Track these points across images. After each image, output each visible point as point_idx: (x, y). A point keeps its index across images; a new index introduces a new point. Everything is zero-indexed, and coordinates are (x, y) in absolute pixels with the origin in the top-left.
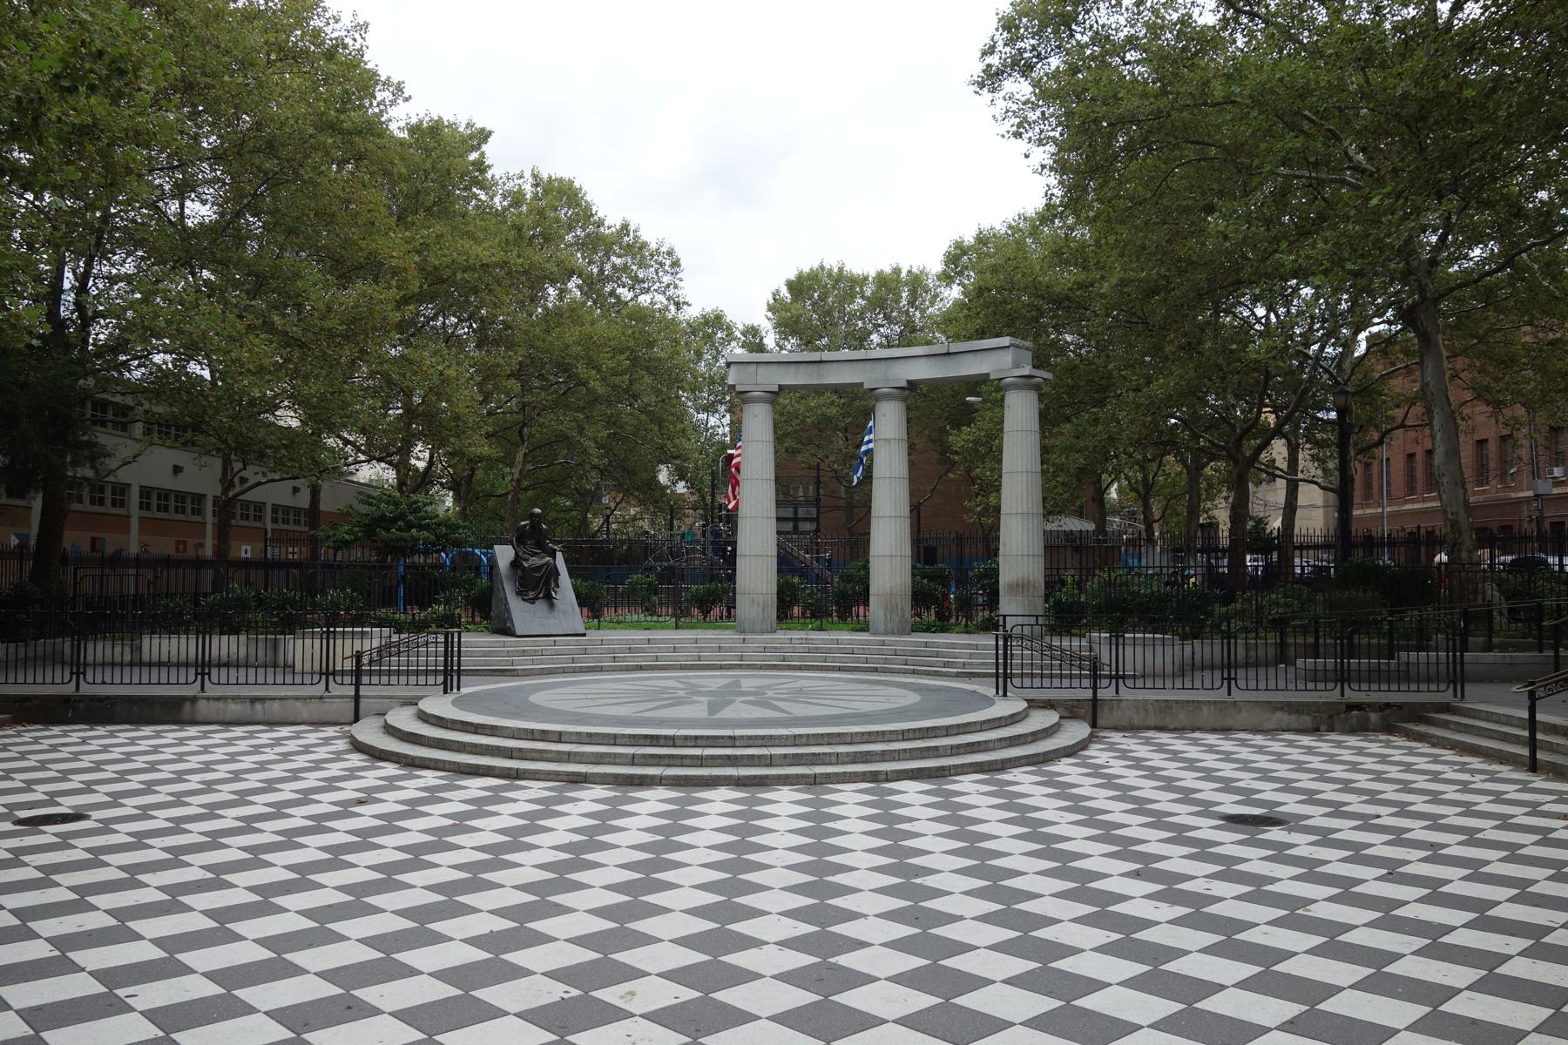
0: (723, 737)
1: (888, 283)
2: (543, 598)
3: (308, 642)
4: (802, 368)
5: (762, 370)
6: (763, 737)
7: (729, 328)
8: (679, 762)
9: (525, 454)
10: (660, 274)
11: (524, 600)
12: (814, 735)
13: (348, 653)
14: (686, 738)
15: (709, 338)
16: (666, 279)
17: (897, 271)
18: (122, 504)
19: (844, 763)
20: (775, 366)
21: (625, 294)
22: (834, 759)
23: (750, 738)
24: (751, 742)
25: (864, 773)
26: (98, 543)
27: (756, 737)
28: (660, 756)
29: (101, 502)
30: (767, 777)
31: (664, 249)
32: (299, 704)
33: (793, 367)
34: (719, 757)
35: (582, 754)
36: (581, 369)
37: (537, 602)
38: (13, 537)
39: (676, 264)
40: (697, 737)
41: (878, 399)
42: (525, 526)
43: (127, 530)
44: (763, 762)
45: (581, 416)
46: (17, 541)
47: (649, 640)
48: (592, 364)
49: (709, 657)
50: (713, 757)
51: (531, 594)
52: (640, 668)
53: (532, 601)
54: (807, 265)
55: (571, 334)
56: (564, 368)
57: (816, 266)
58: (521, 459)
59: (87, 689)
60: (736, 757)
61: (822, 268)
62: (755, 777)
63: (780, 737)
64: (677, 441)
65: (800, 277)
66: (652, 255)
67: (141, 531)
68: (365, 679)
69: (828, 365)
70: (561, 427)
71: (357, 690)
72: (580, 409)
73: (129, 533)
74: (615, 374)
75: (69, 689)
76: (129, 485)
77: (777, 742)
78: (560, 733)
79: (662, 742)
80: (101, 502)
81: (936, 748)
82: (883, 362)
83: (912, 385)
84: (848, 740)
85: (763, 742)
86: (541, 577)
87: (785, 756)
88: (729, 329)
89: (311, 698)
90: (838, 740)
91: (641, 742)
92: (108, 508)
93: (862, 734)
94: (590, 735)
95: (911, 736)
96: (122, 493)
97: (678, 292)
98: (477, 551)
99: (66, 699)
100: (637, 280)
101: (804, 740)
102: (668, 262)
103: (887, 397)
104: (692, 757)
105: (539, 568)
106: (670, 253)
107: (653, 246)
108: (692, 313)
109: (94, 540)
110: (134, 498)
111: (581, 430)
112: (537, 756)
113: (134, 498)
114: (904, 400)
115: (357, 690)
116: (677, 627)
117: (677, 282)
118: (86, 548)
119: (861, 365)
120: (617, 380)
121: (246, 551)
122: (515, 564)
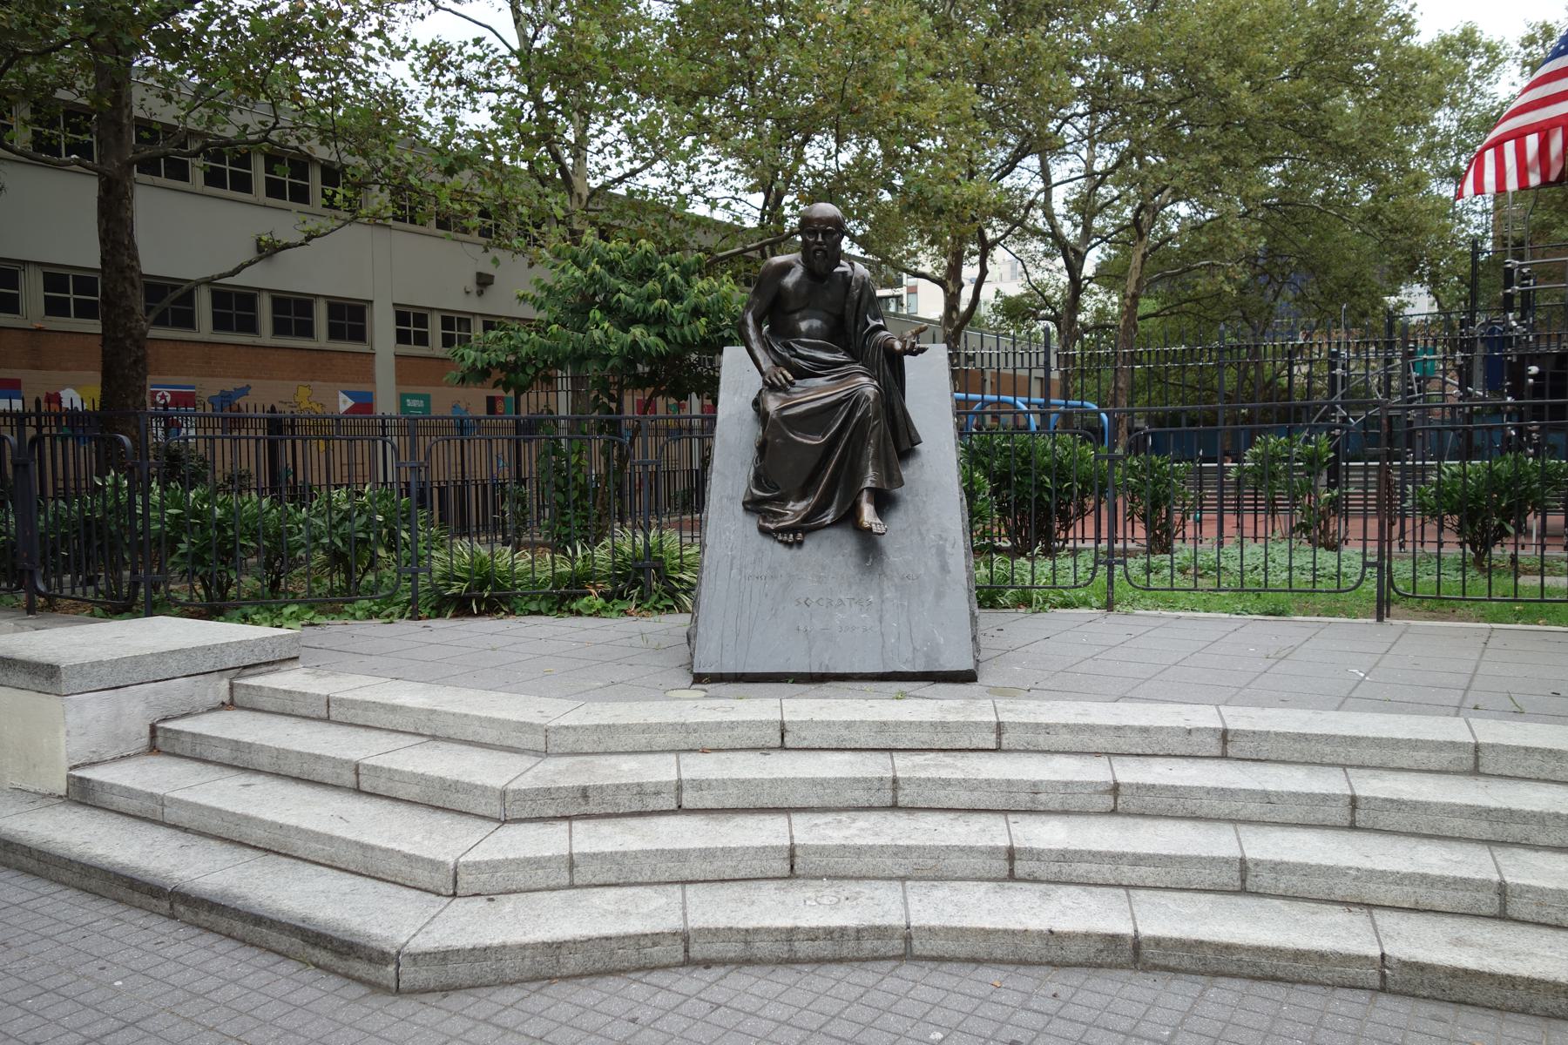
2: (833, 524)
9: (1145, 256)
11: (764, 531)
37: (811, 544)
38: (342, 397)
42: (786, 269)
46: (350, 403)
47: (1224, 736)
51: (796, 509)
53: (794, 535)
58: (1138, 264)
86: (830, 446)
88: (1493, 54)
108: (1425, 36)
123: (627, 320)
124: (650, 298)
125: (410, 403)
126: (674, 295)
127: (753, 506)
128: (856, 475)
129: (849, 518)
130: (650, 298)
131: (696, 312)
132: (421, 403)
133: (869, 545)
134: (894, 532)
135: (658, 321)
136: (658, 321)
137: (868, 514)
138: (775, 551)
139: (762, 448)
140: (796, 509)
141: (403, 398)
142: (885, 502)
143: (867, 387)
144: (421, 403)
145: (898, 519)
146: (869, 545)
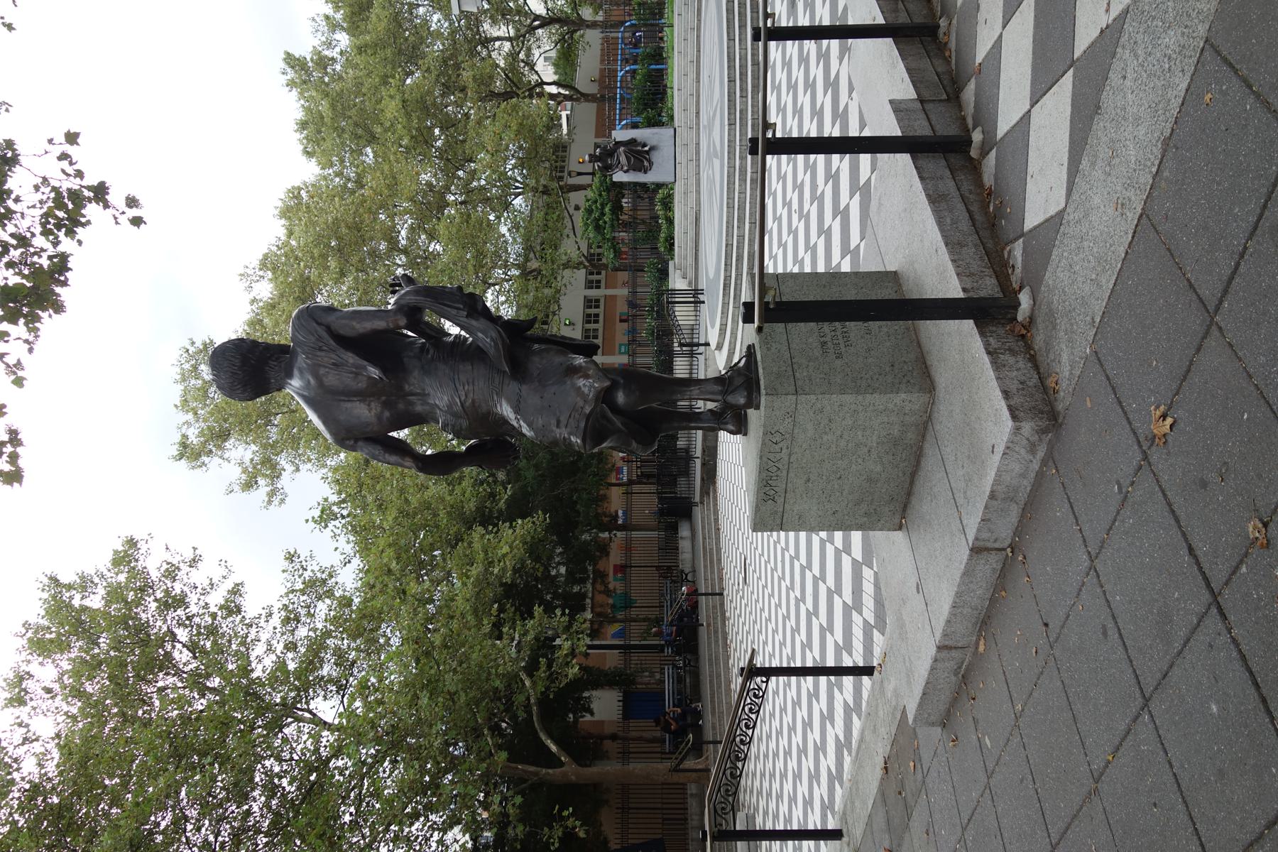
0: (726, 251)
3: (678, 318)
6: (727, 227)
8: (739, 286)
12: (728, 195)
13: (679, 349)
14: (726, 270)
18: (597, 301)
19: (746, 189)
22: (742, 196)
23: (727, 235)
24: (730, 234)
25: (751, 189)
26: (623, 318)
27: (727, 231)
28: (735, 295)
29: (597, 315)
30: (749, 252)
32: (709, 370)
34: (737, 265)
35: (732, 329)
40: (726, 265)
42: (598, 166)
43: (615, 297)
44: (741, 241)
49: (692, 52)
50: (737, 269)
51: (646, 163)
52: (698, 113)
53: (651, 163)
59: (699, 453)
60: (737, 256)
62: (748, 259)
63: (728, 217)
67: (615, 287)
68: (695, 340)
71: (702, 345)
73: (616, 296)
75: (698, 463)
76: (585, 297)
77: (731, 219)
78: (721, 325)
79: (728, 282)
80: (597, 315)
81: (741, 111)
84: (732, 170)
85: (730, 227)
86: (634, 156)
87: (738, 227)
89: (706, 364)
90: (732, 177)
91: (727, 291)
92: (601, 311)
93: (729, 158)
94: (722, 313)
95: (733, 117)
96: (590, 301)
98: (620, 74)
99: (703, 465)
101: (731, 201)
104: (736, 279)
109: (621, 321)
110: (593, 293)
112: (732, 345)
113: (593, 293)
115: (702, 345)
116: (672, 26)
118: (625, 325)
121: (625, 202)
123: (603, 214)
124: (597, 207)
125: (623, 350)
126: (596, 202)
127: (645, 172)
128: (639, 151)
129: (647, 152)
130: (597, 207)
131: (600, 195)
132: (623, 347)
133: (652, 148)
134: (651, 142)
135: (603, 206)
136: (603, 206)
137: (646, 149)
138: (654, 167)
139: (634, 170)
140: (646, 163)
141: (620, 353)
142: (645, 145)
143: (622, 149)
144: (623, 347)
145: (648, 142)
146: (652, 148)
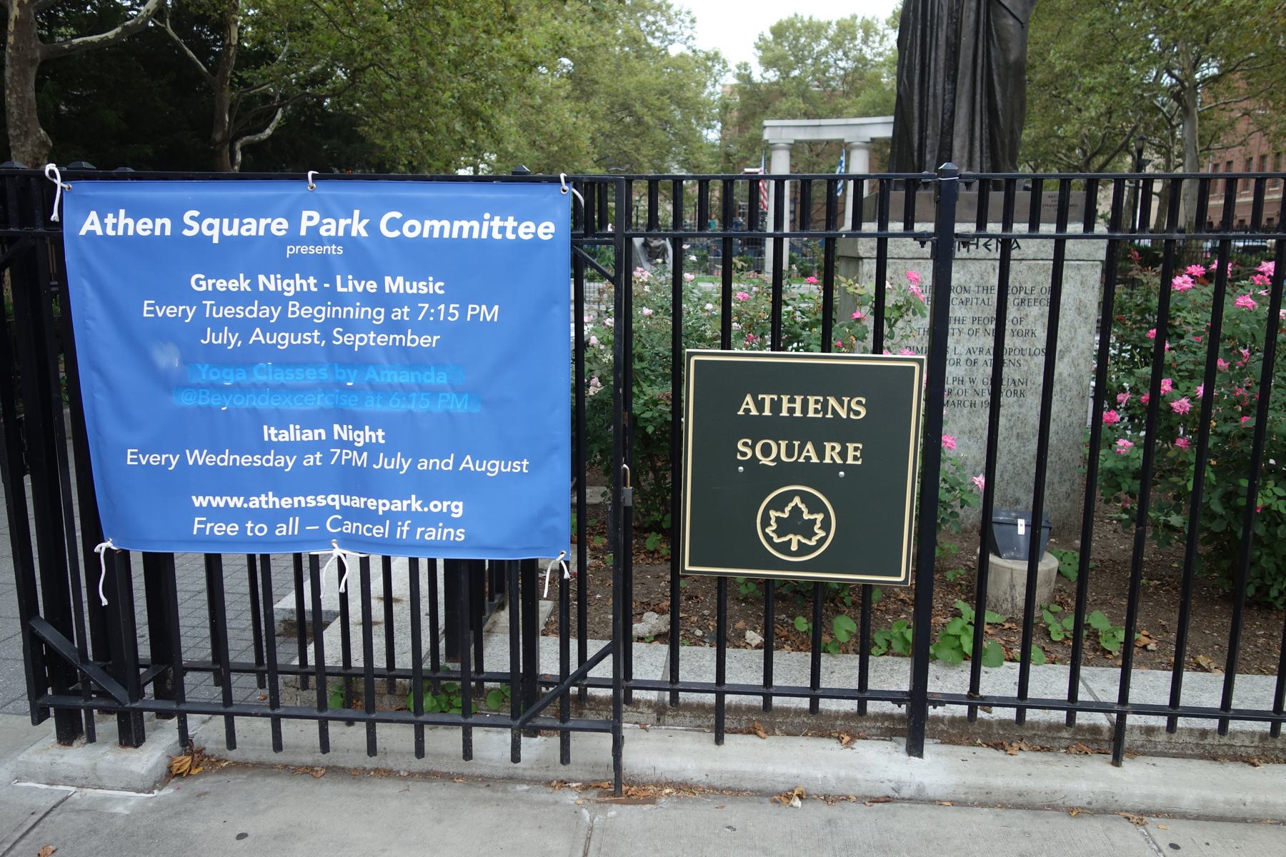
1: (846, 30)
4: (809, 129)
5: (785, 130)
7: (724, 62)
10: (683, 29)
15: (708, 69)
16: (687, 32)
17: (854, 17)
20: (791, 129)
21: (656, 43)
31: (684, 10)
33: (803, 129)
36: (638, 107)
39: (693, 21)
41: (852, 148)
45: (638, 140)
48: (644, 102)
54: (784, 15)
55: (629, 83)
56: (626, 107)
57: (792, 15)
61: (796, 15)
64: (696, 155)
65: (780, 24)
66: (676, 15)
69: (824, 128)
70: (625, 149)
72: (637, 136)
74: (660, 109)
82: (856, 127)
83: (873, 140)
97: (694, 42)
100: (666, 34)
102: (688, 19)
103: (857, 147)
105: (658, 247)
106: (688, 13)
107: (675, 8)
111: (638, 150)
114: (868, 149)
117: (695, 35)
119: (843, 128)
120: (659, 113)
122: (645, 245)
